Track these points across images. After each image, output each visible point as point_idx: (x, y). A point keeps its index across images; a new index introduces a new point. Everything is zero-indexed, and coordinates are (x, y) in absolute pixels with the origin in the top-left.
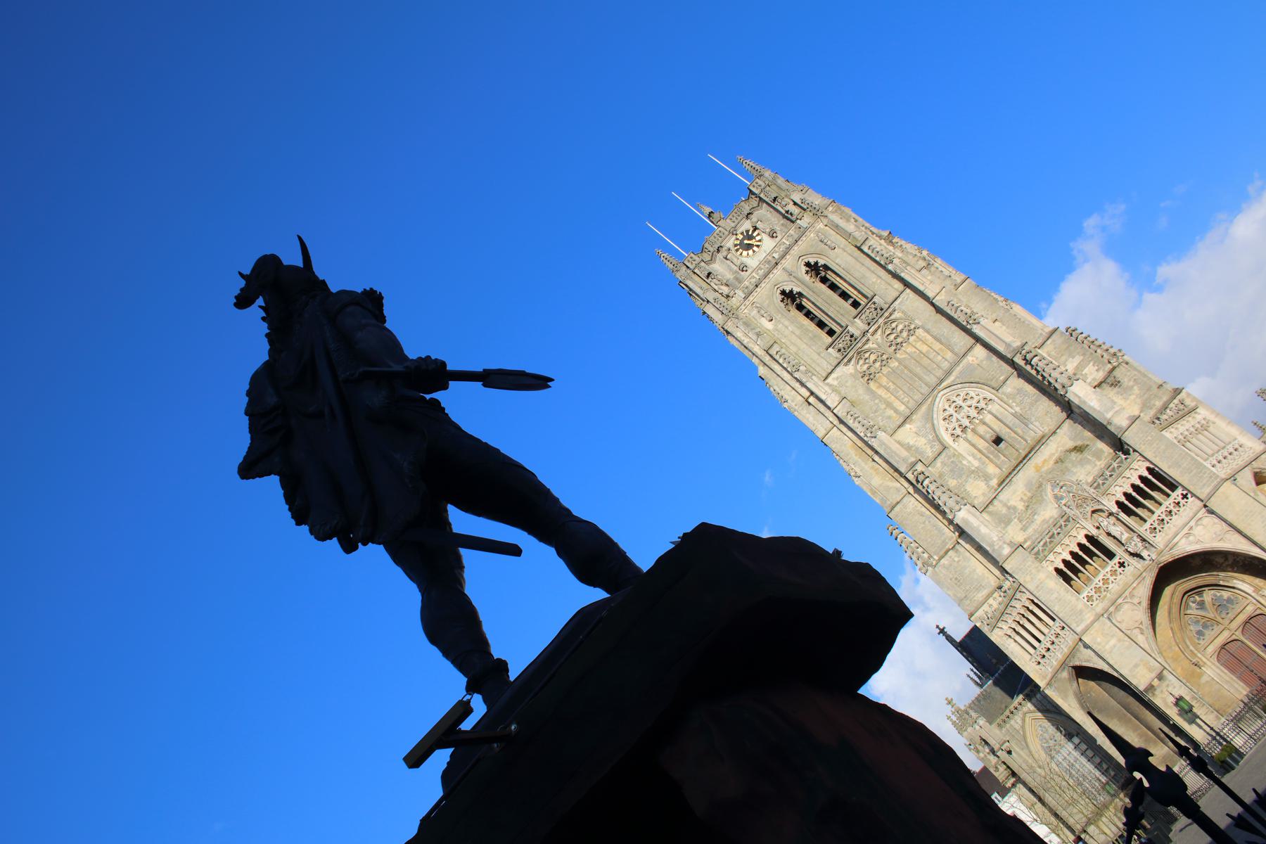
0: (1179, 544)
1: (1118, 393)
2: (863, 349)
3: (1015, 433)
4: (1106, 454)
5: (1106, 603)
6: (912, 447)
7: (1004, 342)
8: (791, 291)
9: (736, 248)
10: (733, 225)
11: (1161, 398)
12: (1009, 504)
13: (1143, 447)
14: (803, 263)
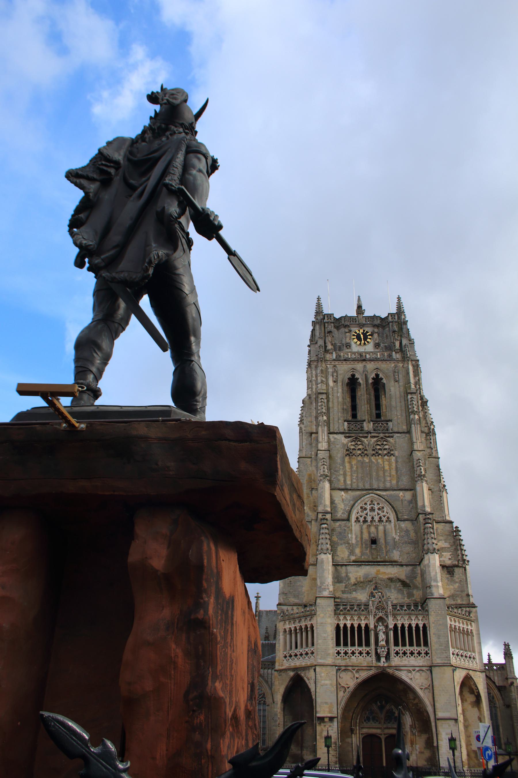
0: (402, 672)
1: (447, 578)
2: (360, 438)
3: (386, 547)
4: (414, 599)
5: (343, 663)
6: (334, 503)
7: (424, 502)
8: (357, 379)
9: (354, 334)
10: (364, 322)
12: (348, 574)
13: (433, 613)
14: (376, 372)
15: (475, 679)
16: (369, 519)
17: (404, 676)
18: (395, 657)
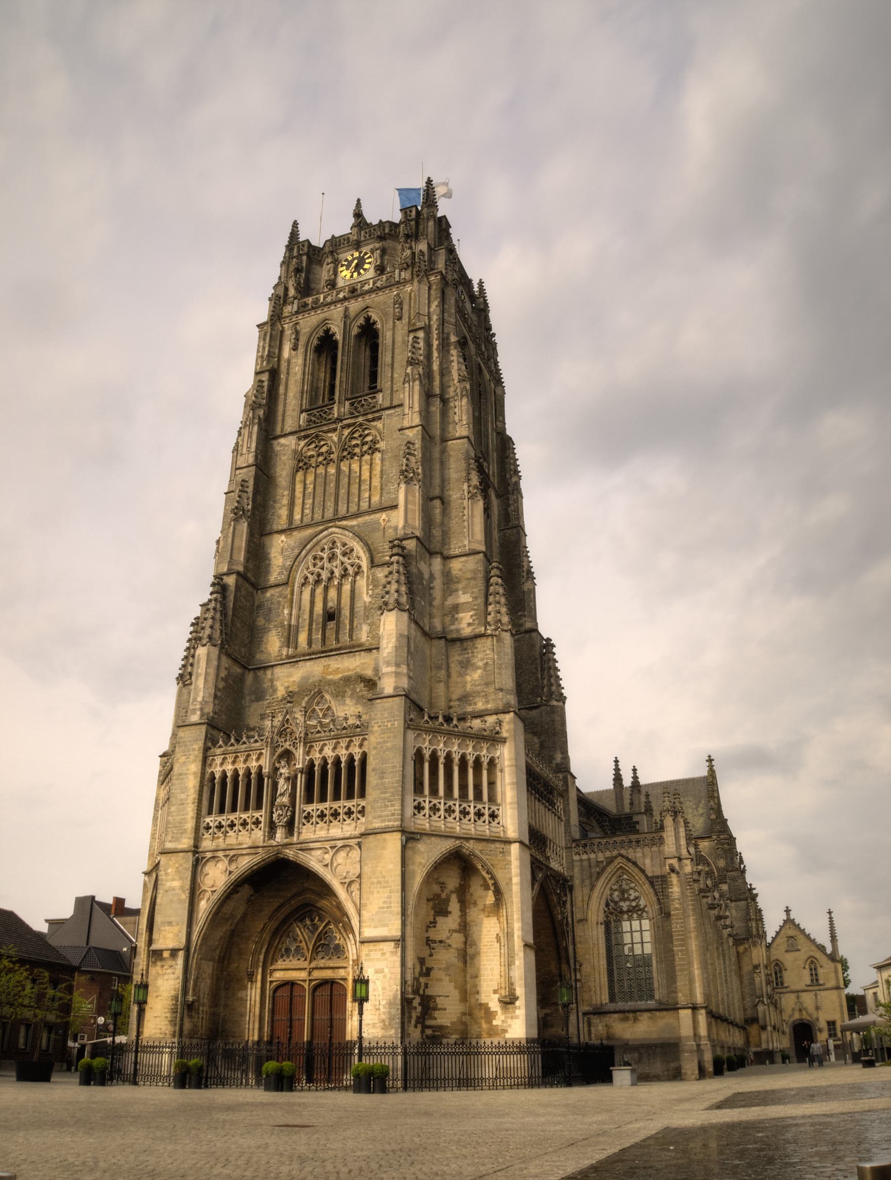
8: (334, 334)
11: (487, 702)
13: (376, 728)
15: (484, 858)
16: (325, 575)
17: (314, 861)
18: (304, 825)
